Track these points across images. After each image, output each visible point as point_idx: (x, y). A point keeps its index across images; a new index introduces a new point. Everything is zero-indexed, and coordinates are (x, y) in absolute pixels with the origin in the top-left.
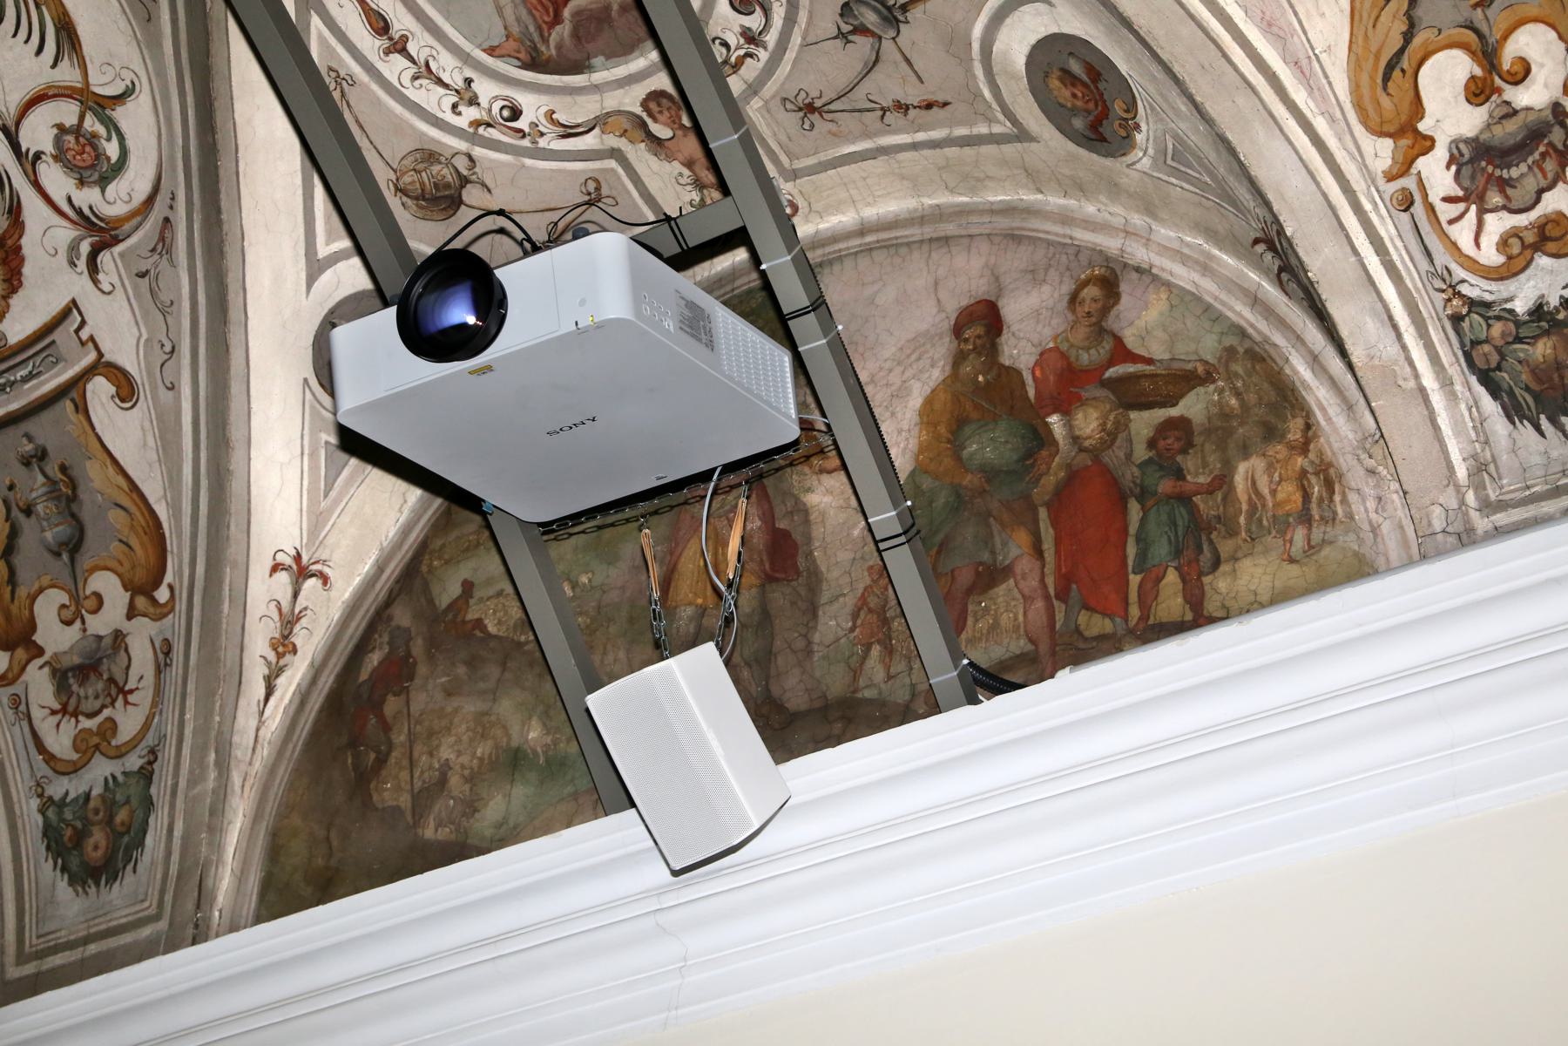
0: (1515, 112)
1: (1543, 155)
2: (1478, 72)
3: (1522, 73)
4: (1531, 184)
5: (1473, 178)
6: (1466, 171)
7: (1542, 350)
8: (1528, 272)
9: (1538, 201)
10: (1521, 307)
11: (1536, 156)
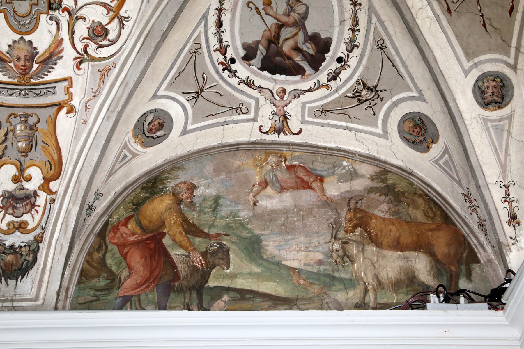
0: (24, 189)
1: (27, 204)
2: (17, 174)
3: (29, 179)
4: (22, 210)
5: (6, 203)
6: (5, 200)
7: (9, 258)
8: (13, 235)
9: (22, 216)
10: (8, 244)
11: (26, 203)
